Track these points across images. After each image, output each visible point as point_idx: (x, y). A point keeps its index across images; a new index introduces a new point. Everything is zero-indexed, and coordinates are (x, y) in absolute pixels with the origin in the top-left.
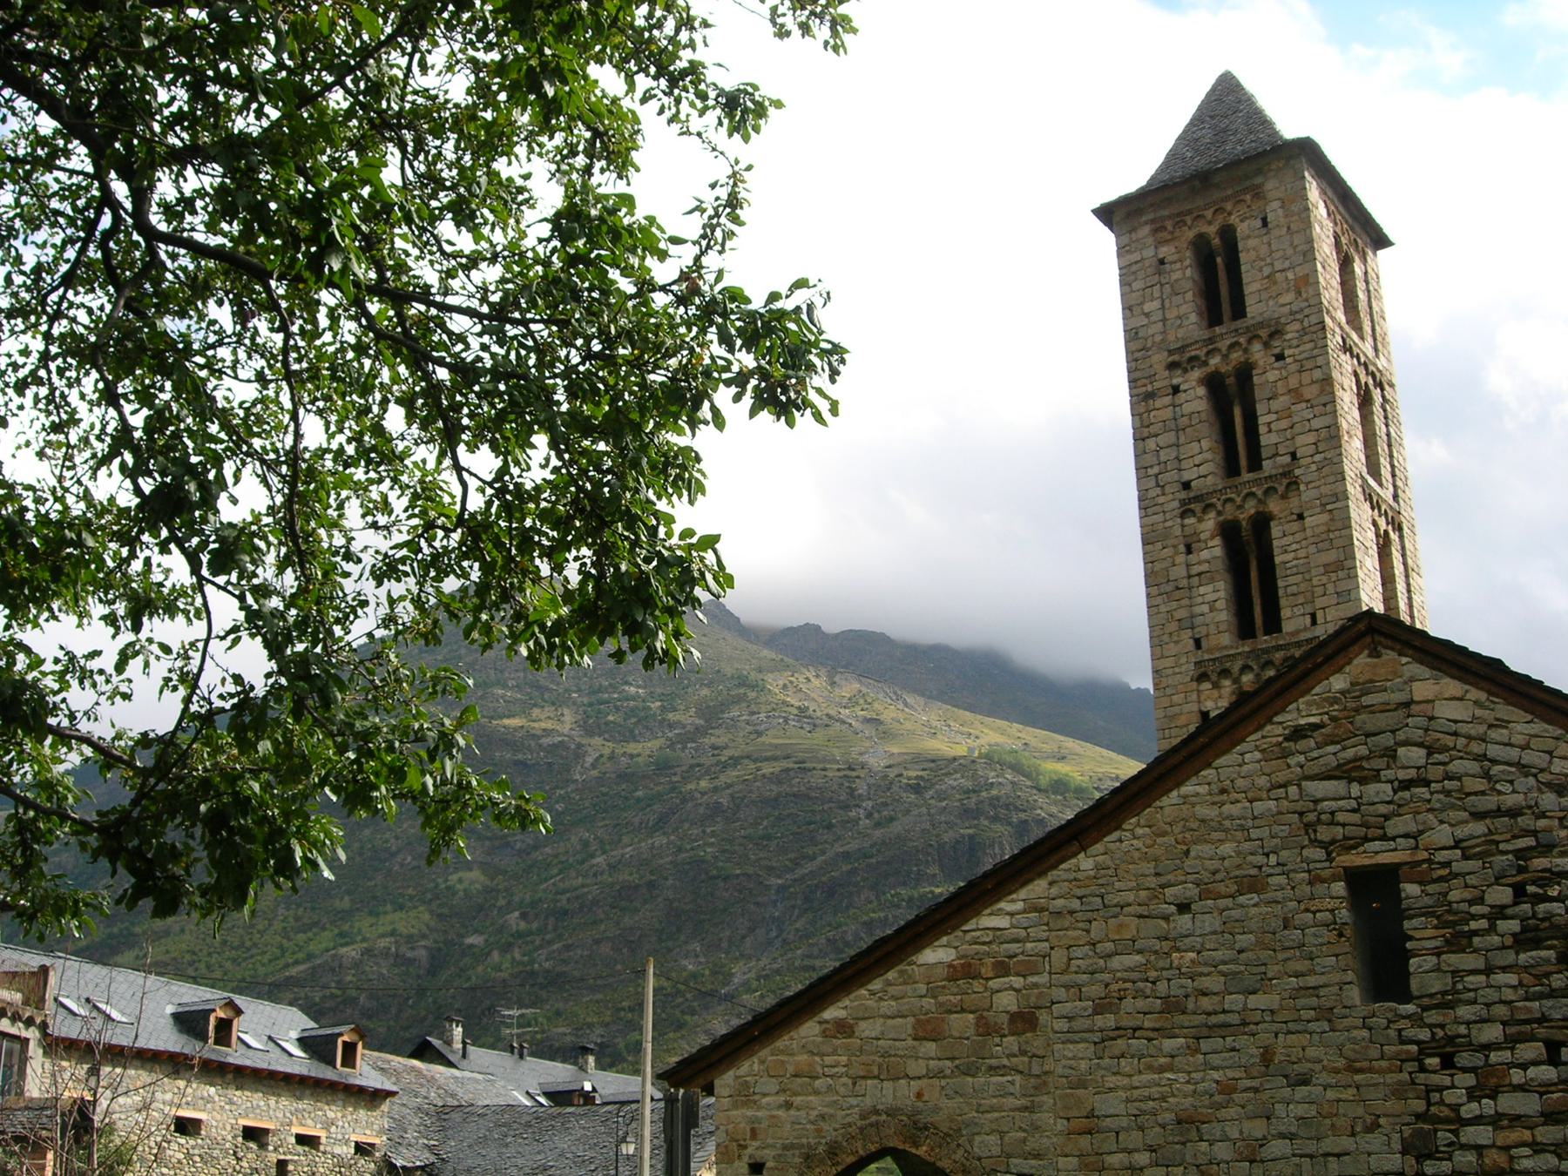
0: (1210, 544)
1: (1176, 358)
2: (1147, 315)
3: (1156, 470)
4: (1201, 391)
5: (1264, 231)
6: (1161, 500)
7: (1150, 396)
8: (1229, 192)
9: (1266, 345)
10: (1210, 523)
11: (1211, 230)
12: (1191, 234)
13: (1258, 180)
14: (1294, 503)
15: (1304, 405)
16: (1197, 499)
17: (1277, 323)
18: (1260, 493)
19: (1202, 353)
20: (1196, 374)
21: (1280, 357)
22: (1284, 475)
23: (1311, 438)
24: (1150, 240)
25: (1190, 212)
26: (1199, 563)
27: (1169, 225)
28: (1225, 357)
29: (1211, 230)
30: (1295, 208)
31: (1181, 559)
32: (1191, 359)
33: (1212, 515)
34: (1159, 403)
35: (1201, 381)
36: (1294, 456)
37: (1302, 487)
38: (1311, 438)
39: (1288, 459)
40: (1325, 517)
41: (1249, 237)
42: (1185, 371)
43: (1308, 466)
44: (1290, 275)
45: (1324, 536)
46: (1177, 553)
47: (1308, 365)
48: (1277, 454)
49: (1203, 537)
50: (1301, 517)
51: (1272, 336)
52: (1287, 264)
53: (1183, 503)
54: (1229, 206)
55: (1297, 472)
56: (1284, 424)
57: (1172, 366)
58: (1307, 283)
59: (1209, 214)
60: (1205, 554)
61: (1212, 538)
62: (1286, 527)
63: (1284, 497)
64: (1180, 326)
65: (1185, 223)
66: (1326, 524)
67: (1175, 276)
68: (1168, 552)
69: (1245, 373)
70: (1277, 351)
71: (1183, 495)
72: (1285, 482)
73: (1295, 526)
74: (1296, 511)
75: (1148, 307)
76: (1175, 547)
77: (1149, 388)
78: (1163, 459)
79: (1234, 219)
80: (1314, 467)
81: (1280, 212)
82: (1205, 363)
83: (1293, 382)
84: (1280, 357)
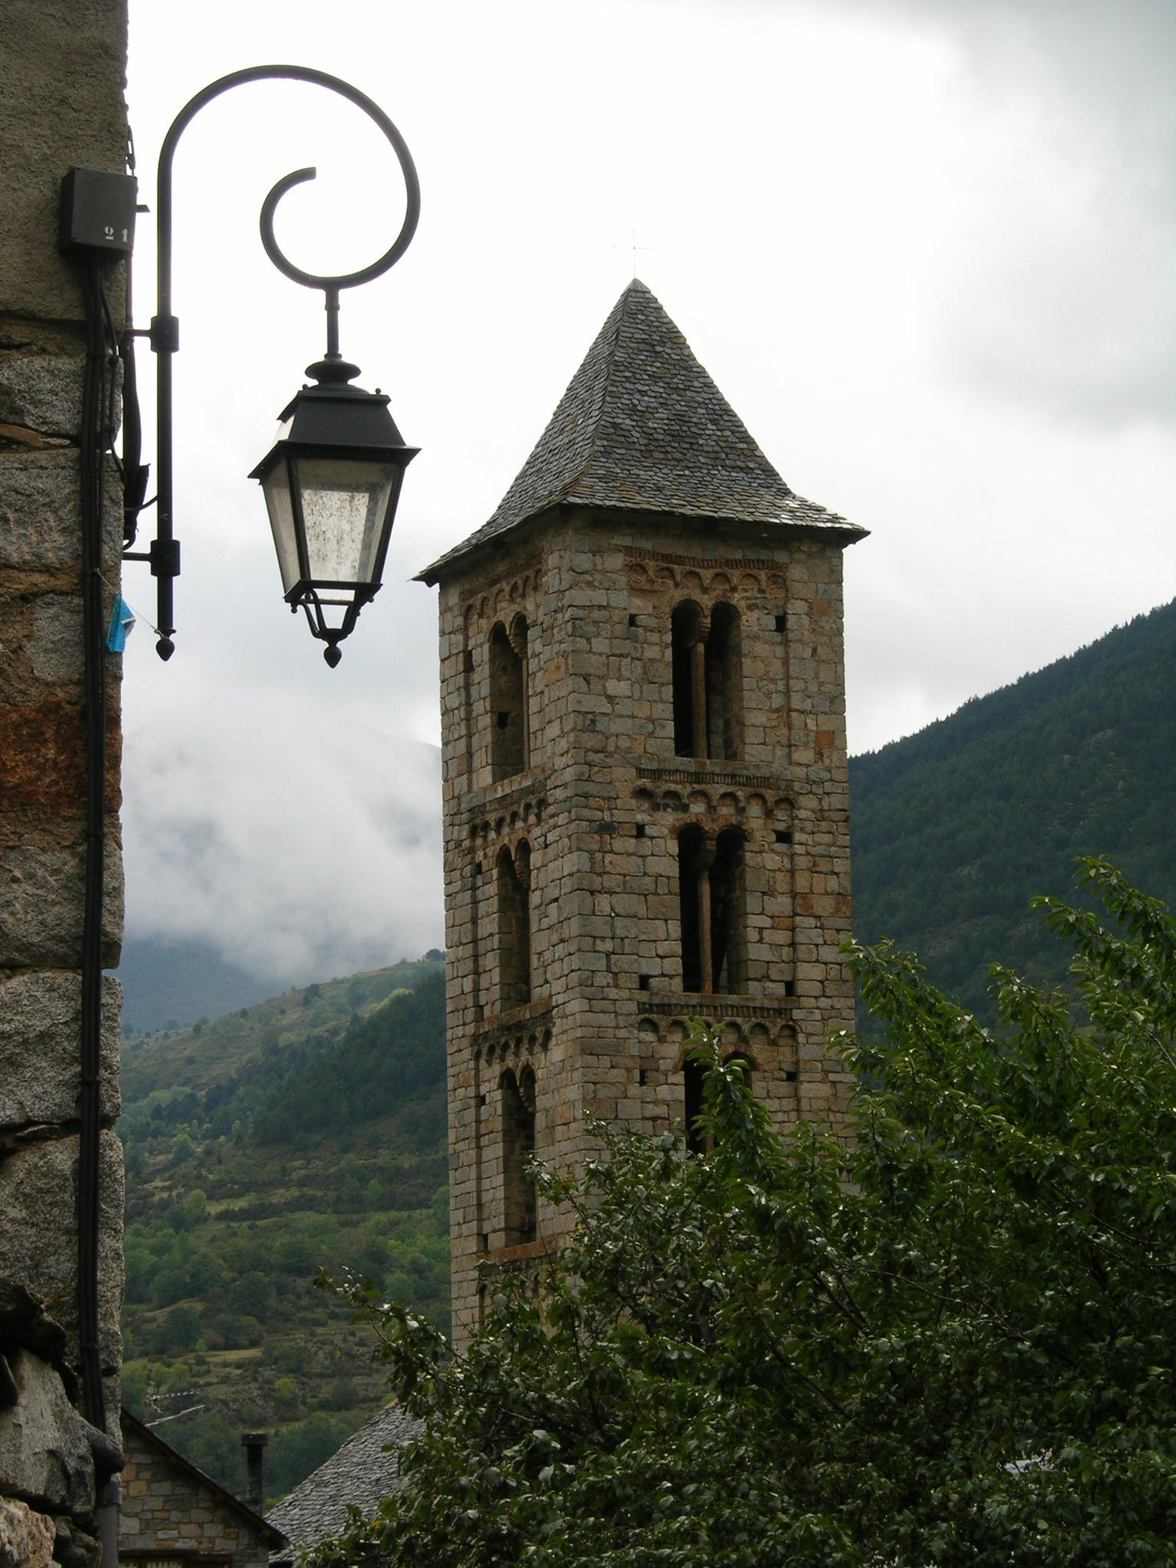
0: (672, 1079)
1: (645, 782)
2: (611, 699)
3: (608, 946)
4: (674, 847)
5: (778, 638)
6: (613, 993)
7: (607, 829)
8: (739, 556)
9: (769, 814)
10: (671, 1051)
11: (707, 602)
12: (678, 595)
13: (781, 557)
14: (785, 1054)
15: (812, 922)
16: (664, 1008)
17: (789, 788)
18: (746, 1027)
19: (685, 790)
20: (669, 819)
21: (784, 837)
22: (779, 1012)
23: (817, 972)
24: (622, 580)
25: (680, 560)
26: (655, 1102)
27: (651, 565)
28: (711, 808)
29: (707, 602)
30: (826, 624)
31: (634, 1090)
32: (670, 794)
33: (678, 1037)
34: (619, 844)
35: (673, 830)
36: (790, 987)
37: (801, 1038)
38: (817, 972)
39: (781, 989)
40: (826, 1090)
41: (756, 637)
42: (656, 808)
43: (811, 1010)
44: (811, 725)
45: (823, 1114)
46: (630, 1081)
47: (823, 865)
48: (767, 977)
49: (664, 1065)
50: (792, 1077)
51: (779, 802)
52: (807, 705)
53: (643, 1008)
54: (735, 576)
55: (797, 1014)
56: (782, 937)
57: (641, 793)
58: (831, 744)
59: (707, 575)
60: (663, 1092)
61: (675, 1071)
62: (772, 1085)
63: (773, 1043)
64: (651, 734)
65: (672, 576)
66: (827, 1099)
67: (651, 652)
68: (617, 1075)
69: (734, 839)
70: (781, 827)
71: (644, 996)
72: (780, 1022)
73: (784, 1088)
74: (787, 1067)
75: (614, 687)
76: (629, 1070)
77: (607, 818)
78: (619, 932)
79: (737, 599)
80: (817, 1015)
81: (806, 620)
82: (685, 808)
83: (802, 883)
84: (784, 837)
